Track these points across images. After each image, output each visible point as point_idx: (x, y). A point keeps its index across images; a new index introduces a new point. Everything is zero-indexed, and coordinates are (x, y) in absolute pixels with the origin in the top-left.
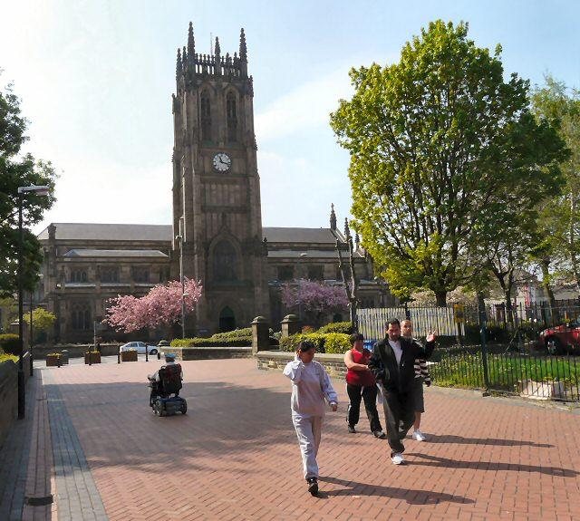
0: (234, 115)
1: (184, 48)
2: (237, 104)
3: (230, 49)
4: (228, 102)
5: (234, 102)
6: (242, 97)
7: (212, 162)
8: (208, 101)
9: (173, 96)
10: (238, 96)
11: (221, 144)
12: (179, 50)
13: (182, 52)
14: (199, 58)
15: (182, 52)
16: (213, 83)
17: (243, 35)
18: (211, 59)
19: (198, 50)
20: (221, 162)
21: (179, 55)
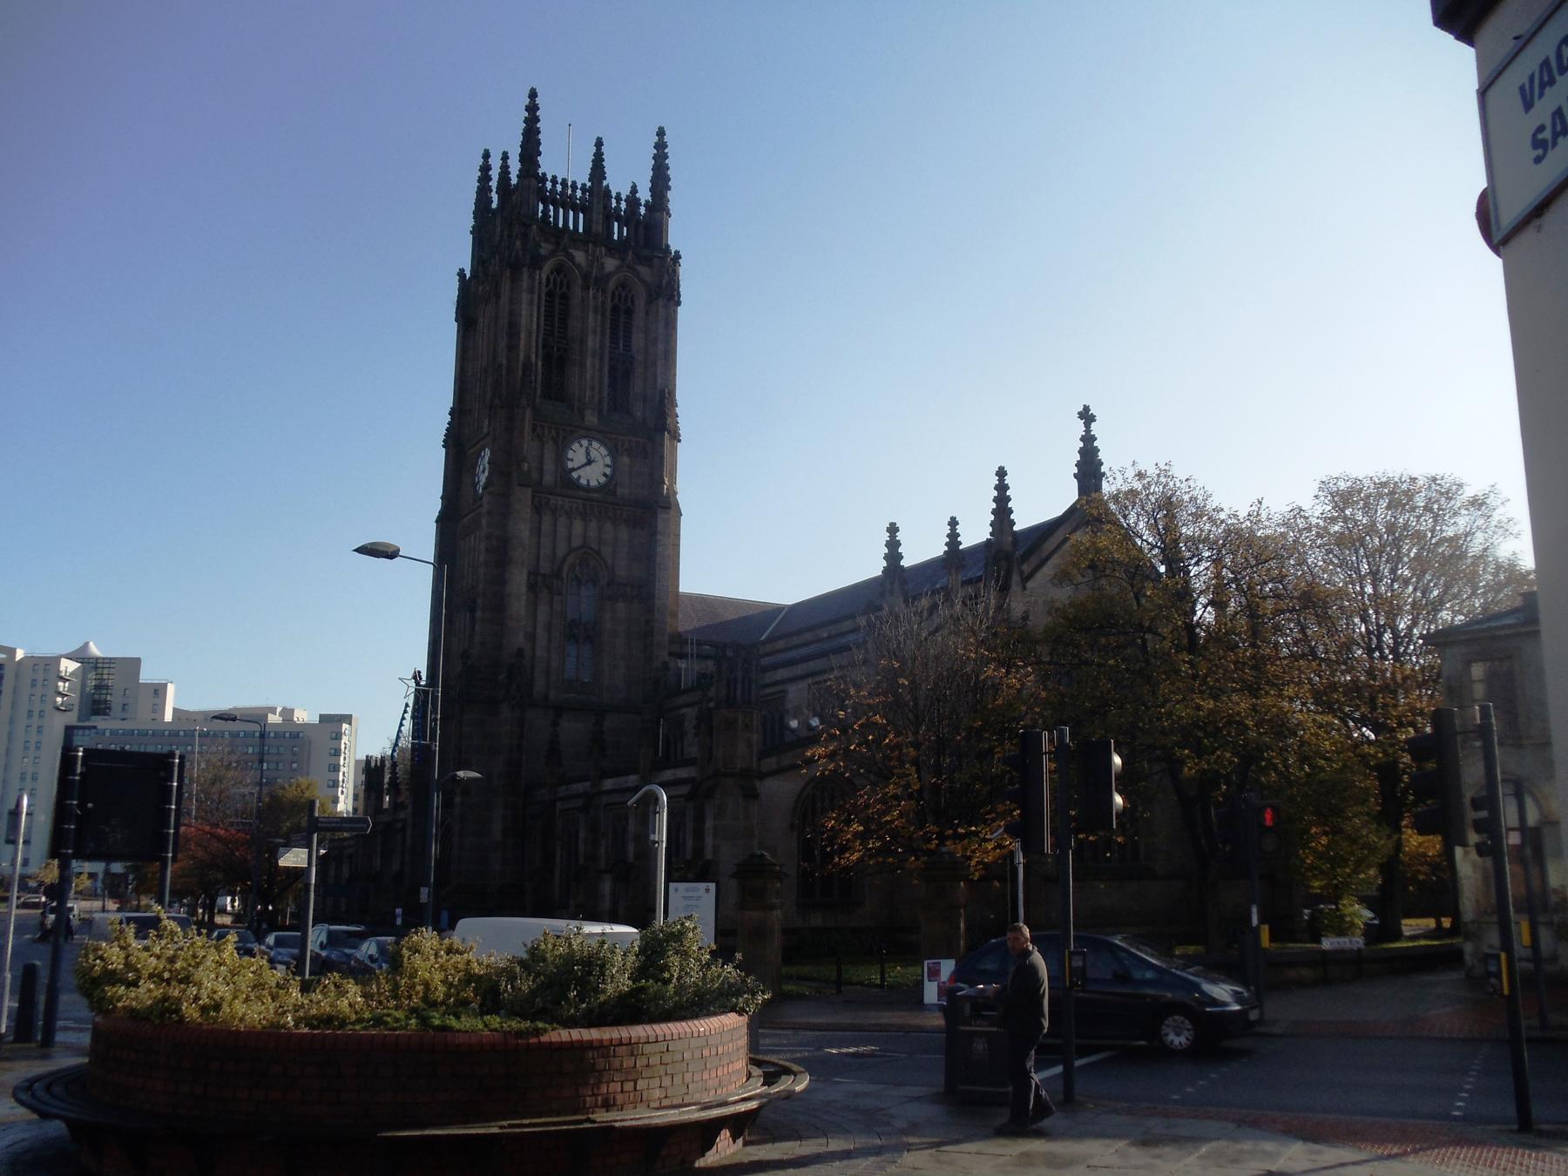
0: (628, 346)
1: (505, 157)
2: (639, 319)
3: (628, 176)
4: (615, 309)
5: (629, 312)
6: (650, 302)
7: (560, 458)
8: (565, 298)
9: (461, 273)
10: (641, 304)
11: (591, 419)
12: (486, 155)
13: (495, 173)
14: (549, 185)
15: (495, 173)
16: (580, 256)
17: (661, 146)
18: (579, 194)
19: (549, 165)
20: (590, 463)
21: (485, 168)
